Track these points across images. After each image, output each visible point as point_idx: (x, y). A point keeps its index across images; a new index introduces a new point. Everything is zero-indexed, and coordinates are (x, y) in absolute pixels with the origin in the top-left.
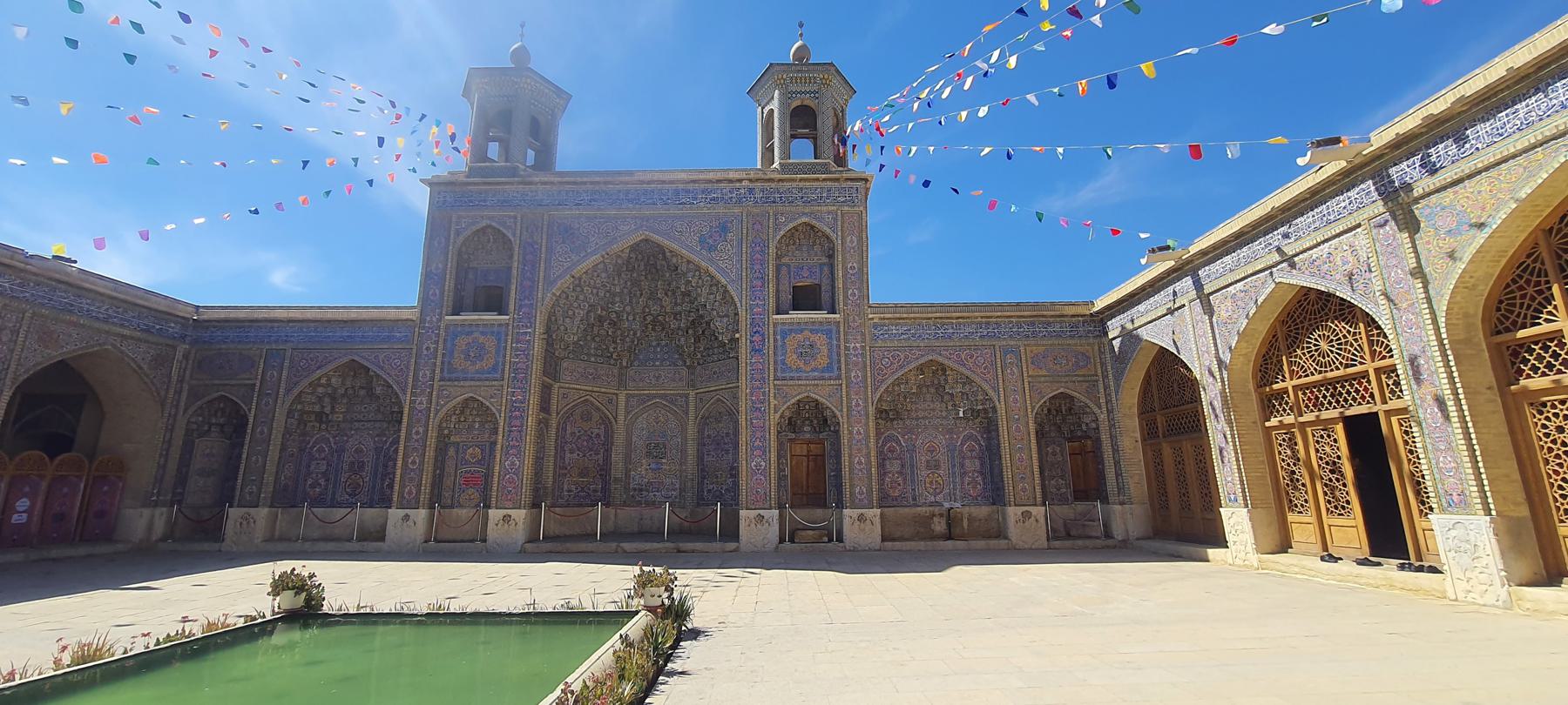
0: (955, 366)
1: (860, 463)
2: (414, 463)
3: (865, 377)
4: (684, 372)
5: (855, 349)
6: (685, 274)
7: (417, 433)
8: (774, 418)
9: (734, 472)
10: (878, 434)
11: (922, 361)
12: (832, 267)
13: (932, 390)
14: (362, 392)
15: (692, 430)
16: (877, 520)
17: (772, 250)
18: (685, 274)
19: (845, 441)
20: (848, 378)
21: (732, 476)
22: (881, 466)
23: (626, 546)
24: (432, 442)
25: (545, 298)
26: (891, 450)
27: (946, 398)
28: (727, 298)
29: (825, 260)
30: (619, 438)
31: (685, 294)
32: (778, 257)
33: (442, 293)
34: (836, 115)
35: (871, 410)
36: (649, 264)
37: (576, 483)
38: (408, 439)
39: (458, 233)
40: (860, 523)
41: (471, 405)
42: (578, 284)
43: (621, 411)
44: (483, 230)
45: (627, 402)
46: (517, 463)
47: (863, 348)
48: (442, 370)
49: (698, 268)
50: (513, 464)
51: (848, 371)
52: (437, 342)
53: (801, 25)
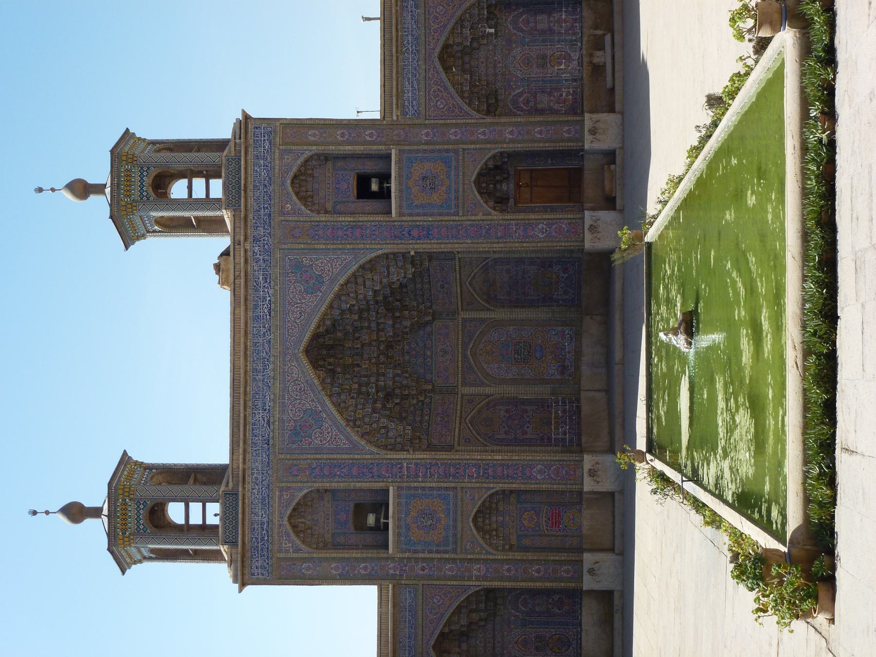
0: (446, 34)
1: (540, 132)
2: (538, 571)
3: (456, 125)
4: (438, 324)
5: (427, 134)
6: (343, 312)
7: (509, 570)
8: (496, 216)
9: (545, 263)
10: (510, 114)
11: (441, 69)
12: (338, 157)
13: (467, 59)
14: (464, 646)
15: (501, 314)
16: (595, 116)
17: (323, 218)
18: (343, 312)
19: (519, 147)
20: (456, 142)
21: (550, 266)
22: (541, 112)
23: (618, 356)
24: (518, 556)
25: (369, 452)
26: (527, 102)
27: (475, 45)
28: (370, 266)
29: (330, 164)
30: (510, 390)
31: (360, 318)
32: (326, 212)
33: (364, 560)
34: (159, 151)
35: (489, 120)
36: (326, 350)
37: (557, 428)
38: (516, 579)
39: (297, 550)
40: (599, 133)
41: (480, 524)
42: (353, 422)
43: (481, 390)
44: (294, 527)
45: (471, 385)
46: (537, 467)
47: (426, 126)
48: (446, 552)
49: (338, 296)
50: (541, 472)
51: (448, 143)
52: (417, 560)
53: (40, 190)
